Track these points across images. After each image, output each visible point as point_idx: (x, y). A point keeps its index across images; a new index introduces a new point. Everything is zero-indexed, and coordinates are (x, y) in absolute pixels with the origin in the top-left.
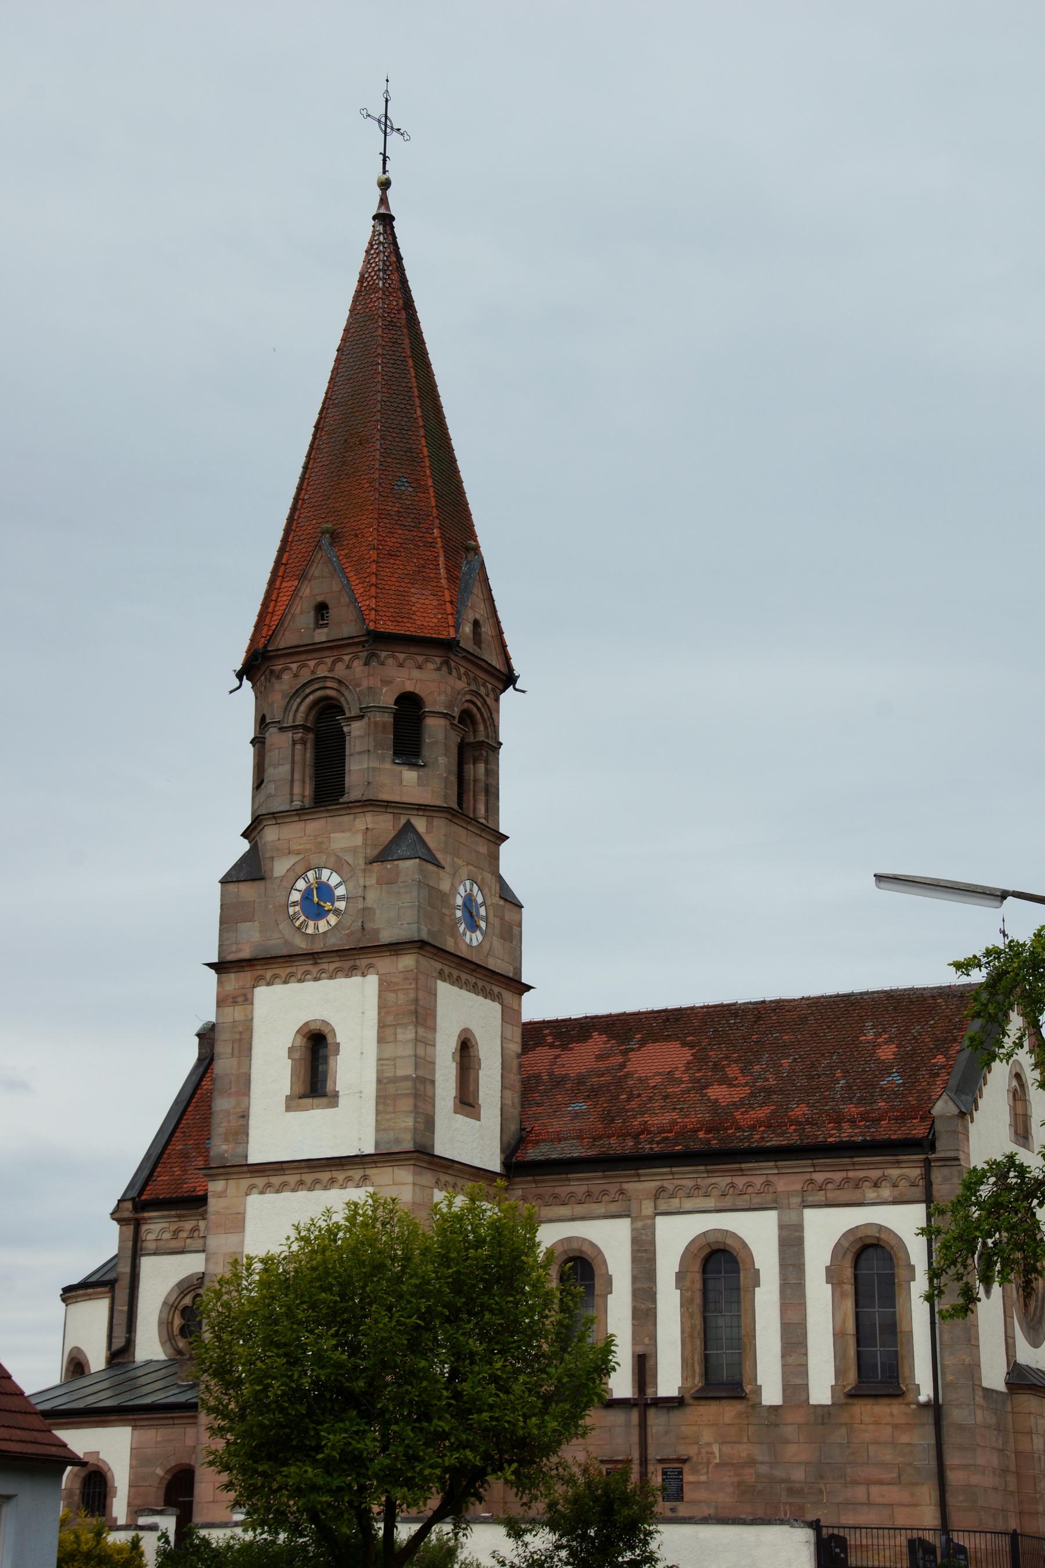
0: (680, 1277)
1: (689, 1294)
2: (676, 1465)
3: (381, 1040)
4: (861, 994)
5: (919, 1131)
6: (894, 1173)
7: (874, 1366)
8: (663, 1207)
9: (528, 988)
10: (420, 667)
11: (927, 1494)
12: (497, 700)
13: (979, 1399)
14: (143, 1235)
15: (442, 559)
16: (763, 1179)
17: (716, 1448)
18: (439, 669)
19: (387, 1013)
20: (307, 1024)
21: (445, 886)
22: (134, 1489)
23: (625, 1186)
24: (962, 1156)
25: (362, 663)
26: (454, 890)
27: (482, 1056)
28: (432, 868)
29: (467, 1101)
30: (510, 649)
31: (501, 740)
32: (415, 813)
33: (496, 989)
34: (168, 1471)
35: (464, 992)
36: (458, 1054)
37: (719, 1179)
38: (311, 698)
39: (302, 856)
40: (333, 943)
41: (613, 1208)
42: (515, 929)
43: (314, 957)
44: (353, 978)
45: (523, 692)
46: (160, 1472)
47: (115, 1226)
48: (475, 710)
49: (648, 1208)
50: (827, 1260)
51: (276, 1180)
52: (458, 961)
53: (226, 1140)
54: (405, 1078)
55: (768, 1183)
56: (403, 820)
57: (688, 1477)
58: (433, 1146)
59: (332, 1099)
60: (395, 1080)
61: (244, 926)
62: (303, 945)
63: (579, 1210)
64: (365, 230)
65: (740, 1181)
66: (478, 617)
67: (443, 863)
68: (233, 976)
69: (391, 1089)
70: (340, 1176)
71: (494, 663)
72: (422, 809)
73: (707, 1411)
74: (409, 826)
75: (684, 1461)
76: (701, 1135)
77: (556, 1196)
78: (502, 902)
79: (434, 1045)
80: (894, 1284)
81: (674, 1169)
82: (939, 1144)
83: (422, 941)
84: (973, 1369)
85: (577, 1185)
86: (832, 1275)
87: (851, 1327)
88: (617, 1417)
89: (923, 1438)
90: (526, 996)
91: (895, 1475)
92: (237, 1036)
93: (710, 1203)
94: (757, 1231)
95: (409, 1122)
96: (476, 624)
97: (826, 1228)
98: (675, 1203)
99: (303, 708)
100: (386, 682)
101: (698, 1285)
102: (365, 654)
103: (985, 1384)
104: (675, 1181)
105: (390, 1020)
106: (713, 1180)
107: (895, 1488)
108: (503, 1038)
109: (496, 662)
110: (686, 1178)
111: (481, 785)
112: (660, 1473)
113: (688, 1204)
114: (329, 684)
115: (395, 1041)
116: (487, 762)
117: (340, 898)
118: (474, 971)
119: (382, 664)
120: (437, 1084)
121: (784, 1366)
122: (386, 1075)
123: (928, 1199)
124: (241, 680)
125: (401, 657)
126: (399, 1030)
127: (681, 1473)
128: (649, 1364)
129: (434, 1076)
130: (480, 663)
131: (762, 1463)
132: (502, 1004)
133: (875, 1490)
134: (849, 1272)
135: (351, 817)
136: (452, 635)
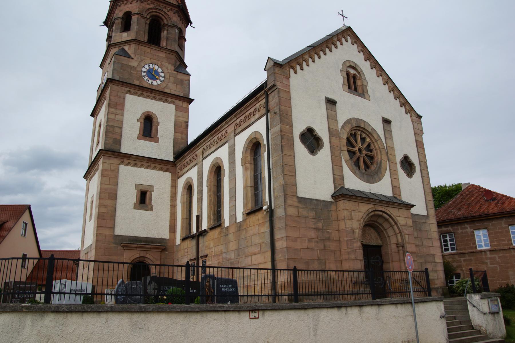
33: (170, 100)
52: (139, 88)
67: (133, 57)
72: (126, 42)
74: (123, 50)
75: (206, 256)
77: (184, 165)
78: (175, 72)
86: (244, 162)
91: (259, 249)
100: (120, 11)
107: (259, 255)
108: (176, 116)
111: (165, 37)
118: (152, 92)
119: (120, 6)
120: (123, 129)
128: (200, 218)
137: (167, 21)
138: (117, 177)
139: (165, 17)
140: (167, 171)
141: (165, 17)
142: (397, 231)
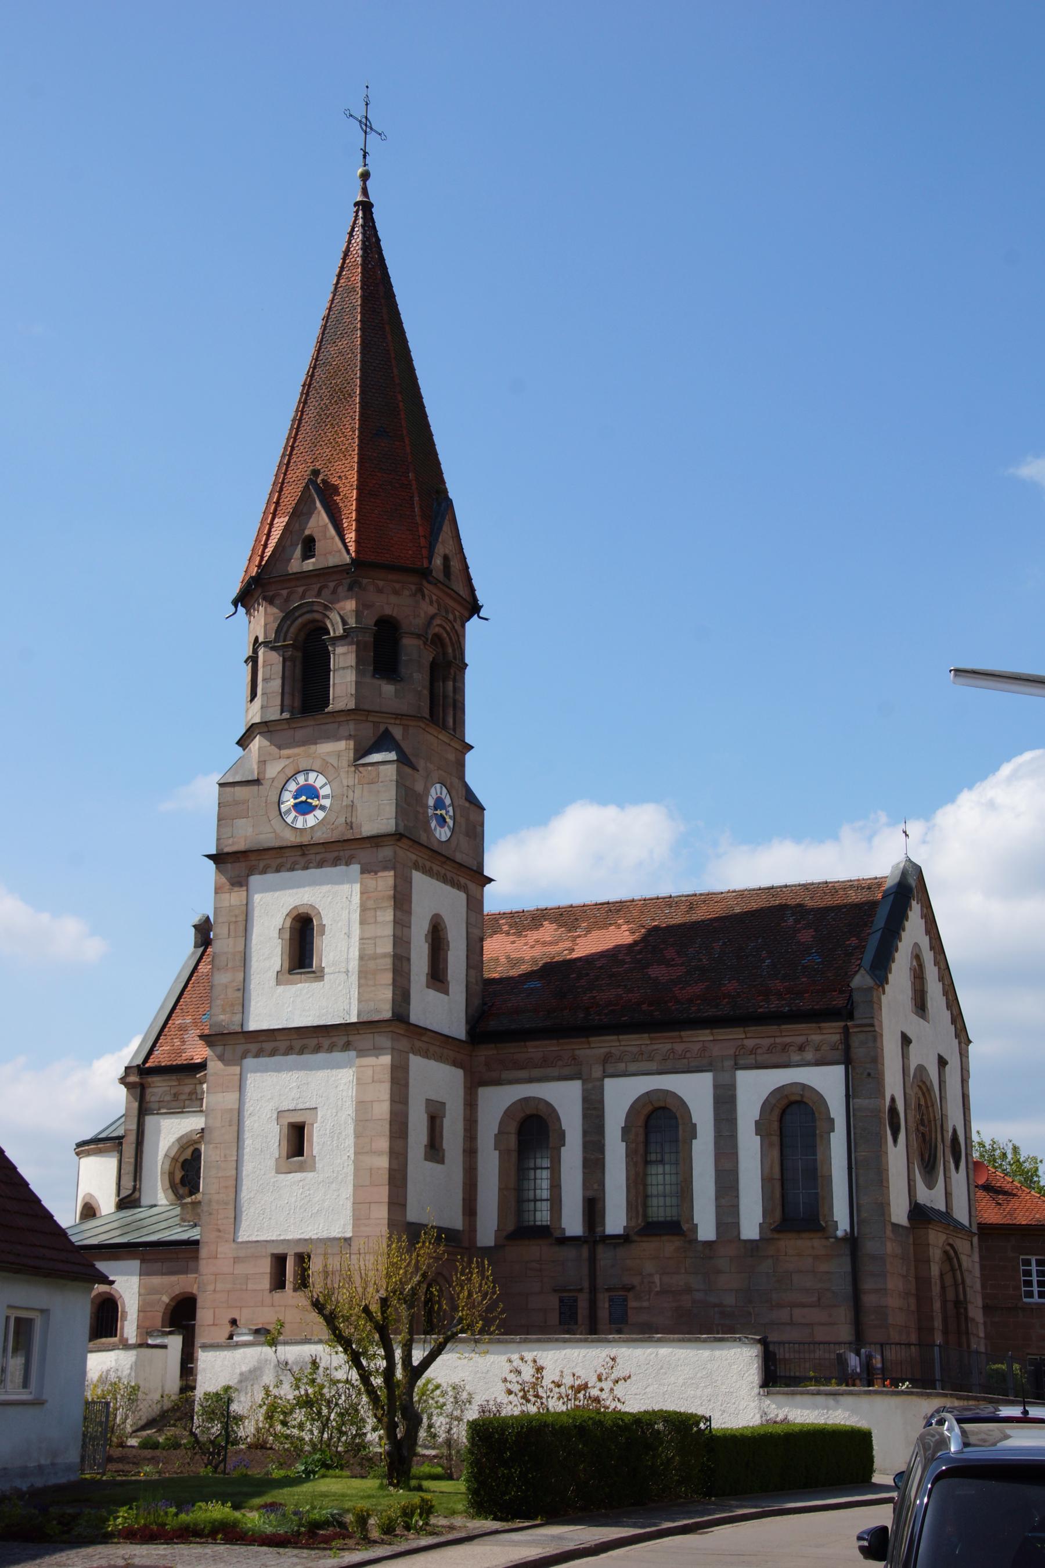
0: (625, 1131)
1: (634, 1145)
2: (621, 1293)
3: (362, 922)
4: (780, 887)
5: (839, 1002)
6: (816, 1038)
7: (796, 1205)
8: (610, 1069)
9: (490, 880)
10: (396, 593)
11: (843, 1315)
12: (463, 626)
13: (889, 1232)
14: (148, 1098)
15: (416, 499)
16: (700, 1045)
17: (657, 1279)
18: (414, 595)
19: (369, 898)
20: (295, 907)
21: (419, 787)
22: (141, 1314)
23: (577, 1052)
24: (876, 1023)
25: (346, 588)
26: (427, 792)
27: (450, 939)
28: (408, 770)
29: (437, 977)
30: (475, 583)
31: (467, 661)
32: (393, 721)
33: (463, 881)
34: (172, 1300)
35: (434, 881)
36: (430, 936)
37: (661, 1046)
38: (300, 620)
39: (291, 760)
40: (320, 836)
41: (566, 1071)
42: (479, 828)
43: (302, 849)
44: (338, 868)
45: (486, 619)
46: (166, 1299)
47: (123, 1090)
48: (445, 635)
49: (597, 1072)
50: (756, 1115)
51: (268, 1046)
53: (224, 1012)
54: (384, 955)
55: (704, 1049)
56: (382, 728)
57: (632, 1304)
58: (409, 1016)
59: (319, 975)
60: (375, 957)
61: (240, 822)
62: (293, 839)
63: (536, 1073)
64: (347, 215)
65: (679, 1047)
66: (447, 552)
68: (229, 865)
69: (372, 965)
70: (326, 1042)
71: (461, 593)
72: (398, 716)
73: (648, 1247)
76: (644, 1007)
78: (467, 804)
79: (410, 927)
80: (814, 1135)
81: (621, 1037)
82: (856, 1014)
83: (400, 834)
84: (883, 1207)
85: (535, 1049)
86: (760, 1127)
87: (777, 1174)
88: (568, 1253)
89: (841, 1266)
90: (488, 888)
91: (815, 1299)
92: (234, 919)
93: (653, 1066)
94: (695, 1090)
95: (388, 994)
96: (446, 559)
97: (755, 1088)
98: (622, 1066)
99: (292, 630)
101: (641, 1138)
102: (348, 581)
103: (894, 1220)
104: (622, 1048)
105: (370, 904)
106: (656, 1047)
109: (463, 592)
110: (632, 1042)
111: (451, 701)
112: (607, 1299)
113: (633, 1067)
114: (316, 608)
115: (376, 922)
116: (455, 681)
117: (326, 797)
118: (444, 863)
121: (717, 1207)
122: (367, 952)
123: (847, 1061)
124: (236, 607)
125: (381, 583)
126: (378, 913)
127: (625, 1300)
129: (409, 954)
130: (449, 591)
131: (698, 1290)
132: (468, 895)
133: (797, 1312)
134: (776, 1125)
135: (336, 725)
136: (425, 565)
137: (454, 651)
138: (407, 1085)
139: (450, 639)
140: (455, 1064)
141: (450, 639)
142: (960, 1281)
